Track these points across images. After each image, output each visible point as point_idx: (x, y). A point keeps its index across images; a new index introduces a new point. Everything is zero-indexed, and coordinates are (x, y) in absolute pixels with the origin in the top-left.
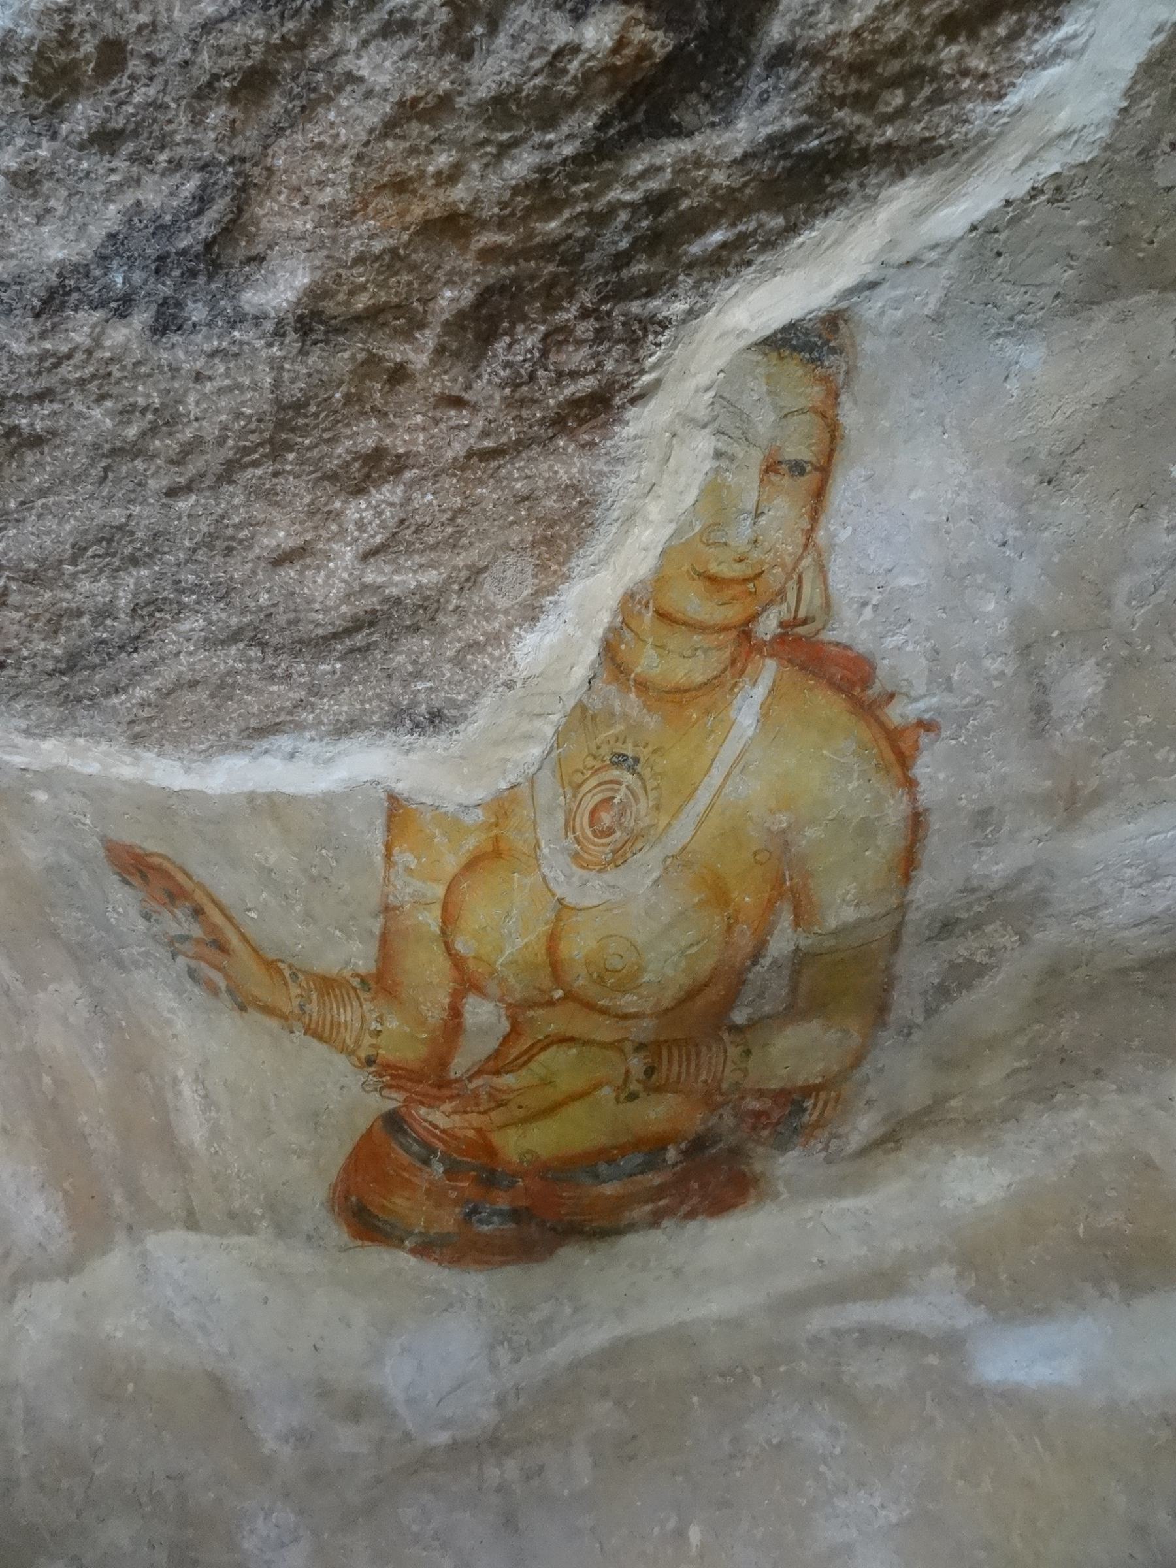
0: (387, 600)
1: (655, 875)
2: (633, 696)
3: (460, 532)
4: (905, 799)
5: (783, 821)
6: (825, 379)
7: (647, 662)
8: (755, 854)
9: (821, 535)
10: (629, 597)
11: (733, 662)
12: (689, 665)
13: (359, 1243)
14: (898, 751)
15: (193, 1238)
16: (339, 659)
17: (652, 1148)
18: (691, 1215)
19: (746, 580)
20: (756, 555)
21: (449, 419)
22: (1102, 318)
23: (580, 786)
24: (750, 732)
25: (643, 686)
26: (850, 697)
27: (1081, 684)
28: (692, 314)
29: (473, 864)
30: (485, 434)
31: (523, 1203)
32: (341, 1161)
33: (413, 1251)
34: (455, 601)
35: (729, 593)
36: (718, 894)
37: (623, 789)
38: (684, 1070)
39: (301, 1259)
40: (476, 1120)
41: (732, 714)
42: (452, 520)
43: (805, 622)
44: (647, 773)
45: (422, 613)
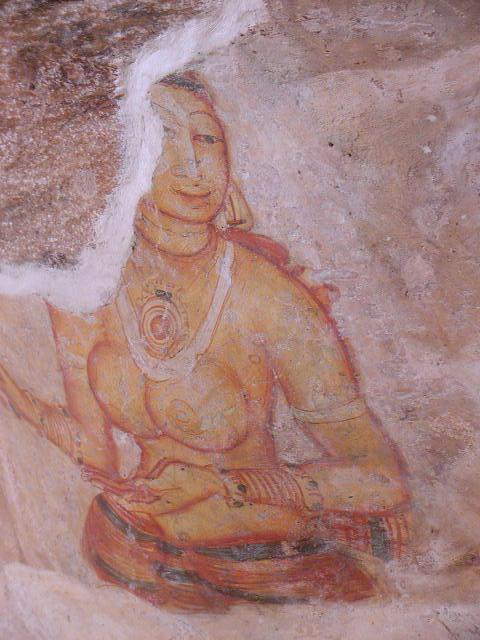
0: (21, 194)
1: (193, 365)
2: (160, 257)
3: (52, 158)
4: (331, 330)
5: (260, 337)
6: (202, 98)
7: (161, 238)
8: (250, 357)
9: (234, 175)
10: (143, 202)
11: (210, 241)
12: (191, 241)
13: (104, 583)
14: (319, 301)
15: (23, 568)
16: (10, 221)
17: (271, 545)
18: (330, 597)
19: (202, 196)
20: (204, 183)
21: (30, 101)
22: (331, 78)
23: (142, 307)
24: (229, 282)
25: (164, 252)
26: (279, 268)
27: (419, 269)
28: (126, 64)
29: (97, 347)
30: (49, 111)
31: (191, 568)
32: (83, 525)
33: (136, 593)
34: (59, 195)
35: (196, 203)
36: (233, 380)
37: (166, 312)
38: (269, 489)
39: (79, 591)
40: (147, 508)
41: (217, 272)
42: (46, 152)
43: (241, 222)
44: (178, 303)
45: (45, 200)
